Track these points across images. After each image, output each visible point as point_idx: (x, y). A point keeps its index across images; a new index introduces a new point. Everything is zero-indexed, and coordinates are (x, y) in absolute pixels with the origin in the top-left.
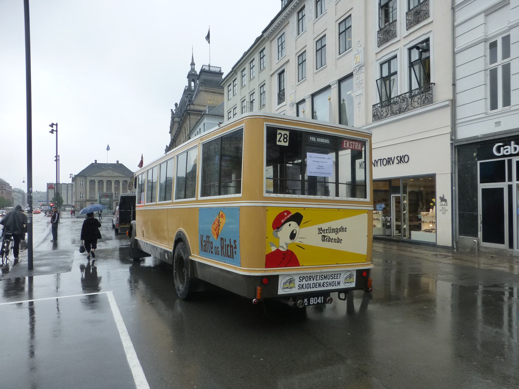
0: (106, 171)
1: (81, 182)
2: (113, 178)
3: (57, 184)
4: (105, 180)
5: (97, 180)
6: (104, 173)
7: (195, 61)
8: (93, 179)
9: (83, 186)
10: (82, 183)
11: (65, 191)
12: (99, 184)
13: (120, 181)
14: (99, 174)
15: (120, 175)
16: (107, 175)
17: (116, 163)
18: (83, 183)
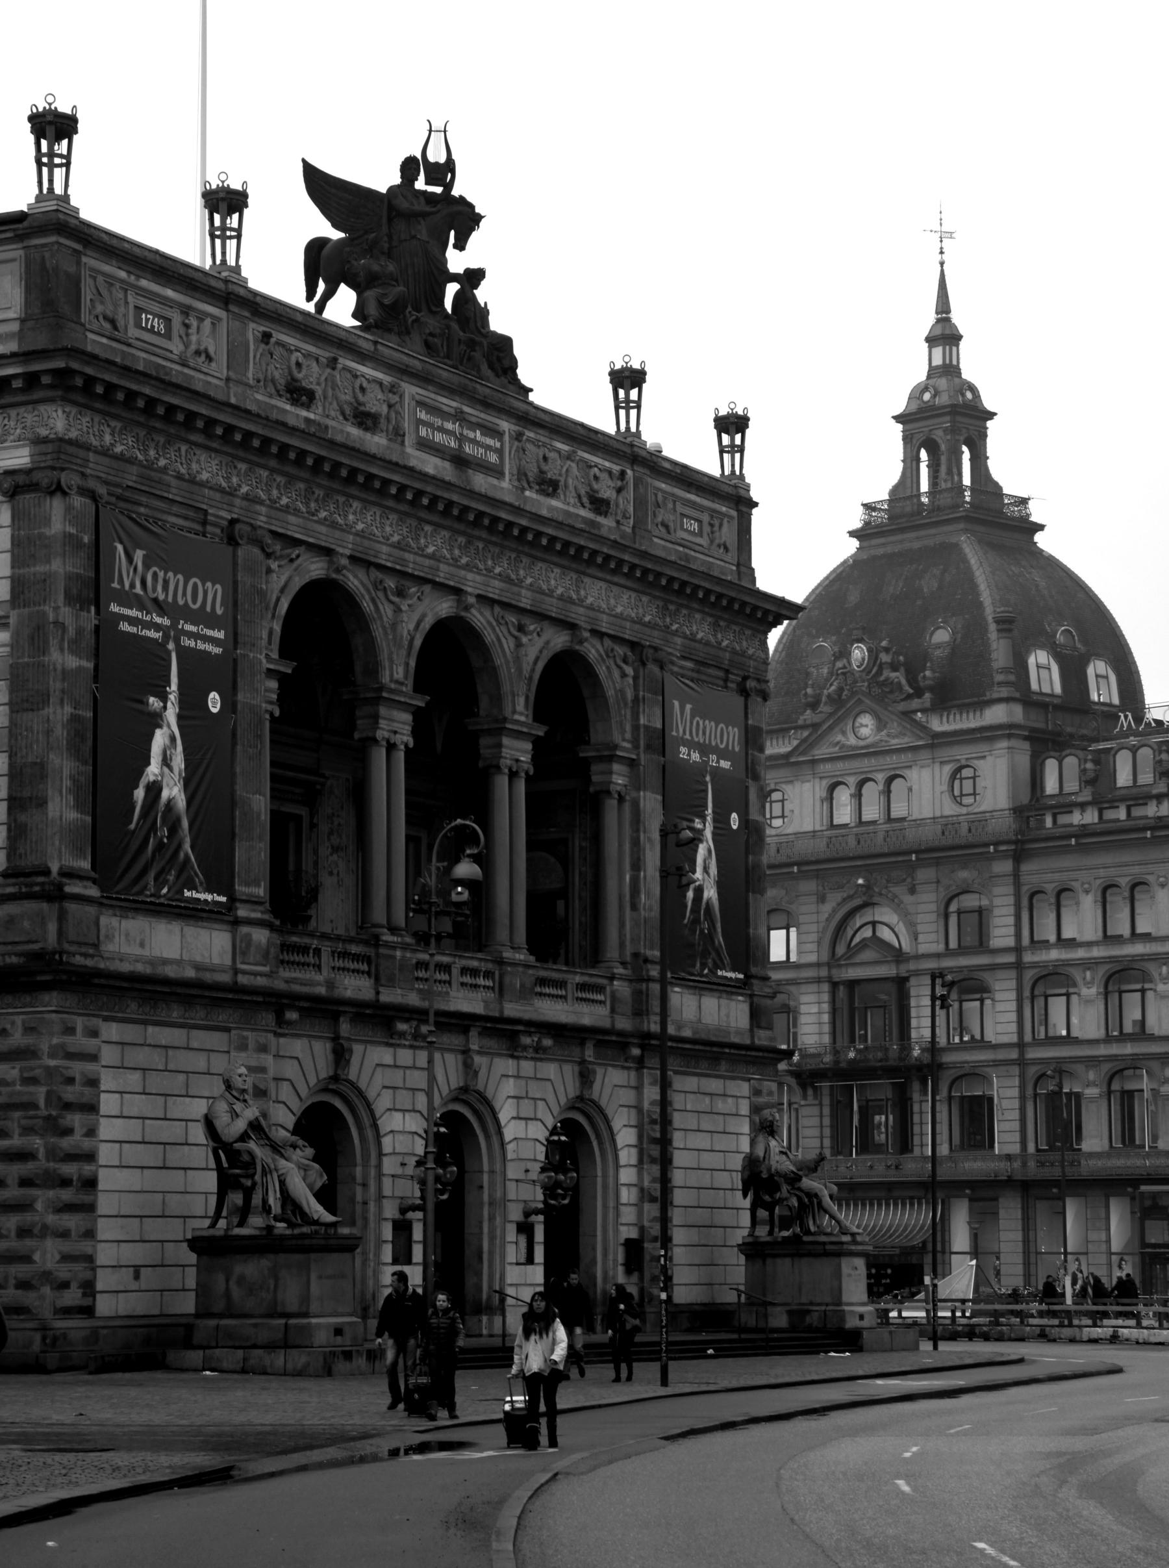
7: (956, 317)
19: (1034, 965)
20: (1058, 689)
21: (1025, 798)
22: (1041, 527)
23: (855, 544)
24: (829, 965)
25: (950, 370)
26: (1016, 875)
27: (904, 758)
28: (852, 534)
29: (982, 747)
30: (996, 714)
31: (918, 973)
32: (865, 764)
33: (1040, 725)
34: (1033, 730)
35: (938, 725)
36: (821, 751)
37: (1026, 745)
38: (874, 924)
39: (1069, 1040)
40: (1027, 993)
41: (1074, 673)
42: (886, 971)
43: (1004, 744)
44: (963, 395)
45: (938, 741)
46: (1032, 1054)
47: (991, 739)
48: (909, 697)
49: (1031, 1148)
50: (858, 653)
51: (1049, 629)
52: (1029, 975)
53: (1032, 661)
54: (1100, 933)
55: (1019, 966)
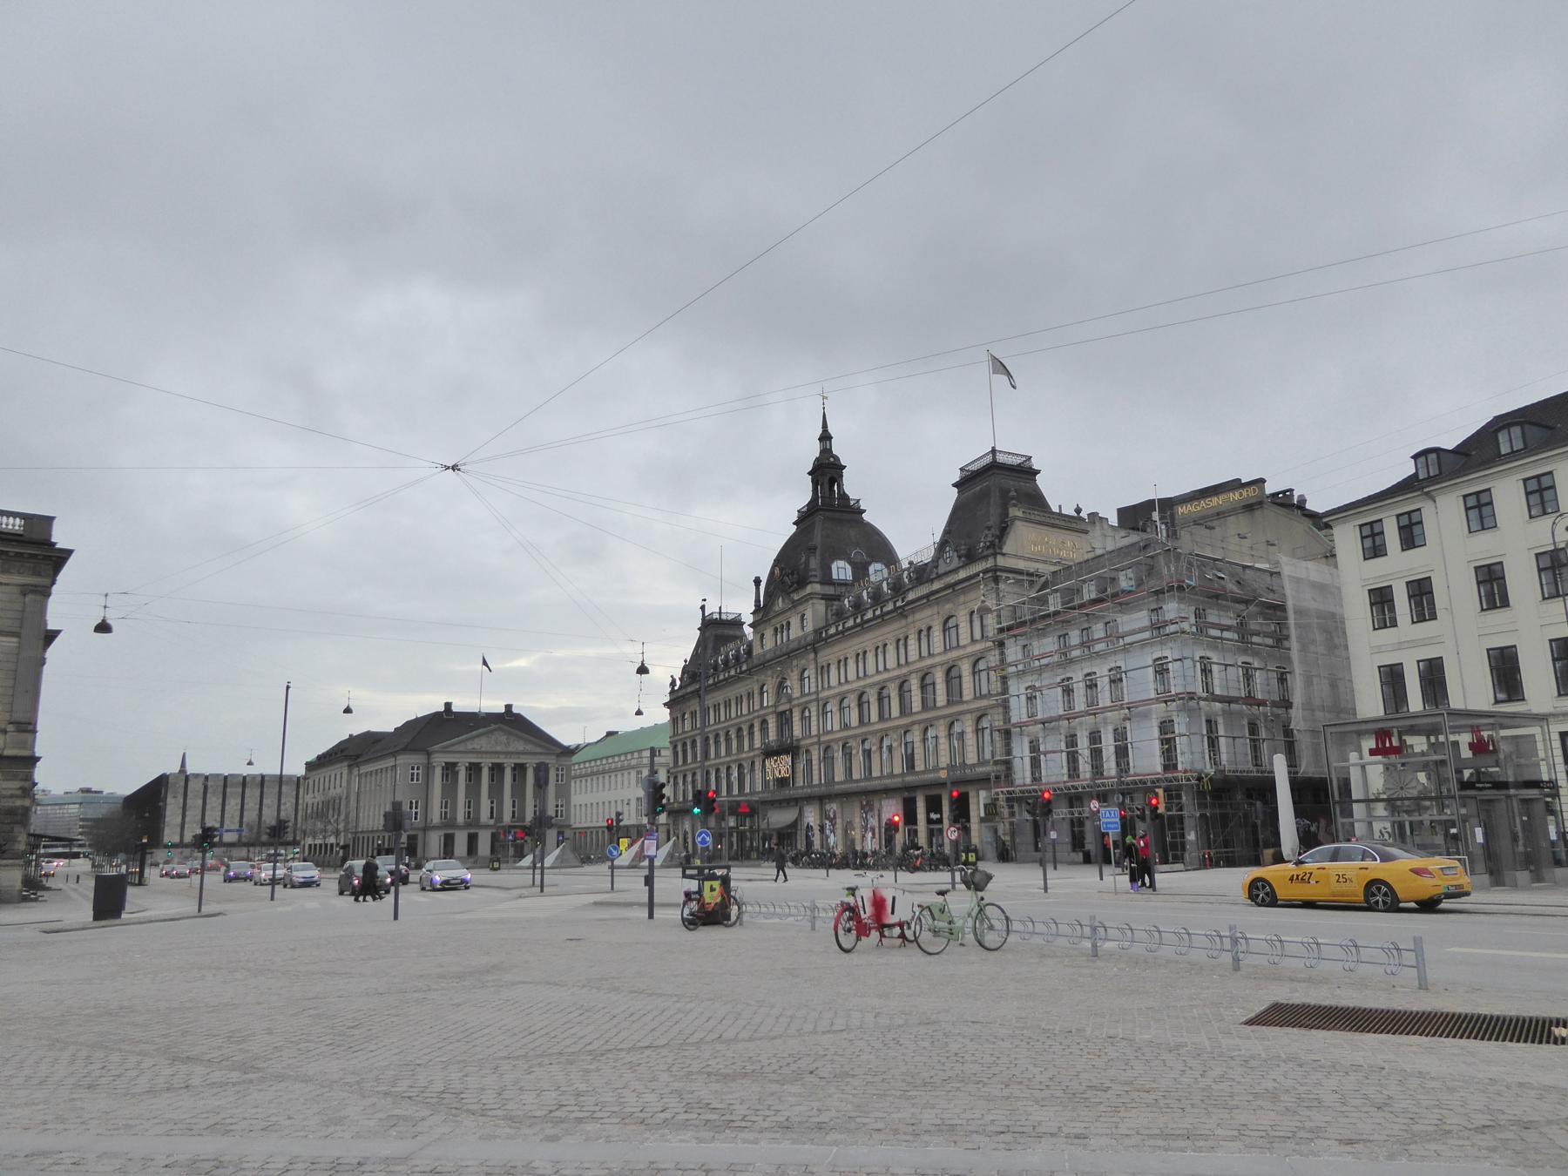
0: (490, 735)
1: (413, 768)
2: (480, 756)
3: (281, 776)
4: (486, 762)
5: (463, 762)
6: (483, 743)
8: (451, 759)
9: (450, 782)
10: (415, 771)
11: (218, 799)
12: (447, 775)
13: (483, 765)
14: (470, 746)
15: (529, 748)
16: (494, 750)
17: (503, 710)
18: (420, 771)
19: (822, 699)
20: (850, 577)
21: (822, 624)
22: (864, 511)
23: (795, 527)
24: (775, 706)
25: (826, 452)
26: (815, 660)
27: (789, 613)
28: (794, 523)
29: (805, 605)
30: (809, 589)
31: (794, 706)
32: (780, 618)
33: (833, 593)
34: (823, 595)
35: (796, 598)
36: (772, 614)
37: (823, 602)
38: (787, 687)
39: (832, 732)
40: (821, 711)
41: (860, 571)
42: (786, 707)
43: (811, 602)
44: (828, 459)
45: (795, 604)
46: (822, 739)
47: (807, 600)
48: (791, 586)
49: (823, 782)
50: (777, 571)
51: (849, 552)
52: (821, 703)
53: (834, 566)
54: (837, 683)
55: (817, 700)
